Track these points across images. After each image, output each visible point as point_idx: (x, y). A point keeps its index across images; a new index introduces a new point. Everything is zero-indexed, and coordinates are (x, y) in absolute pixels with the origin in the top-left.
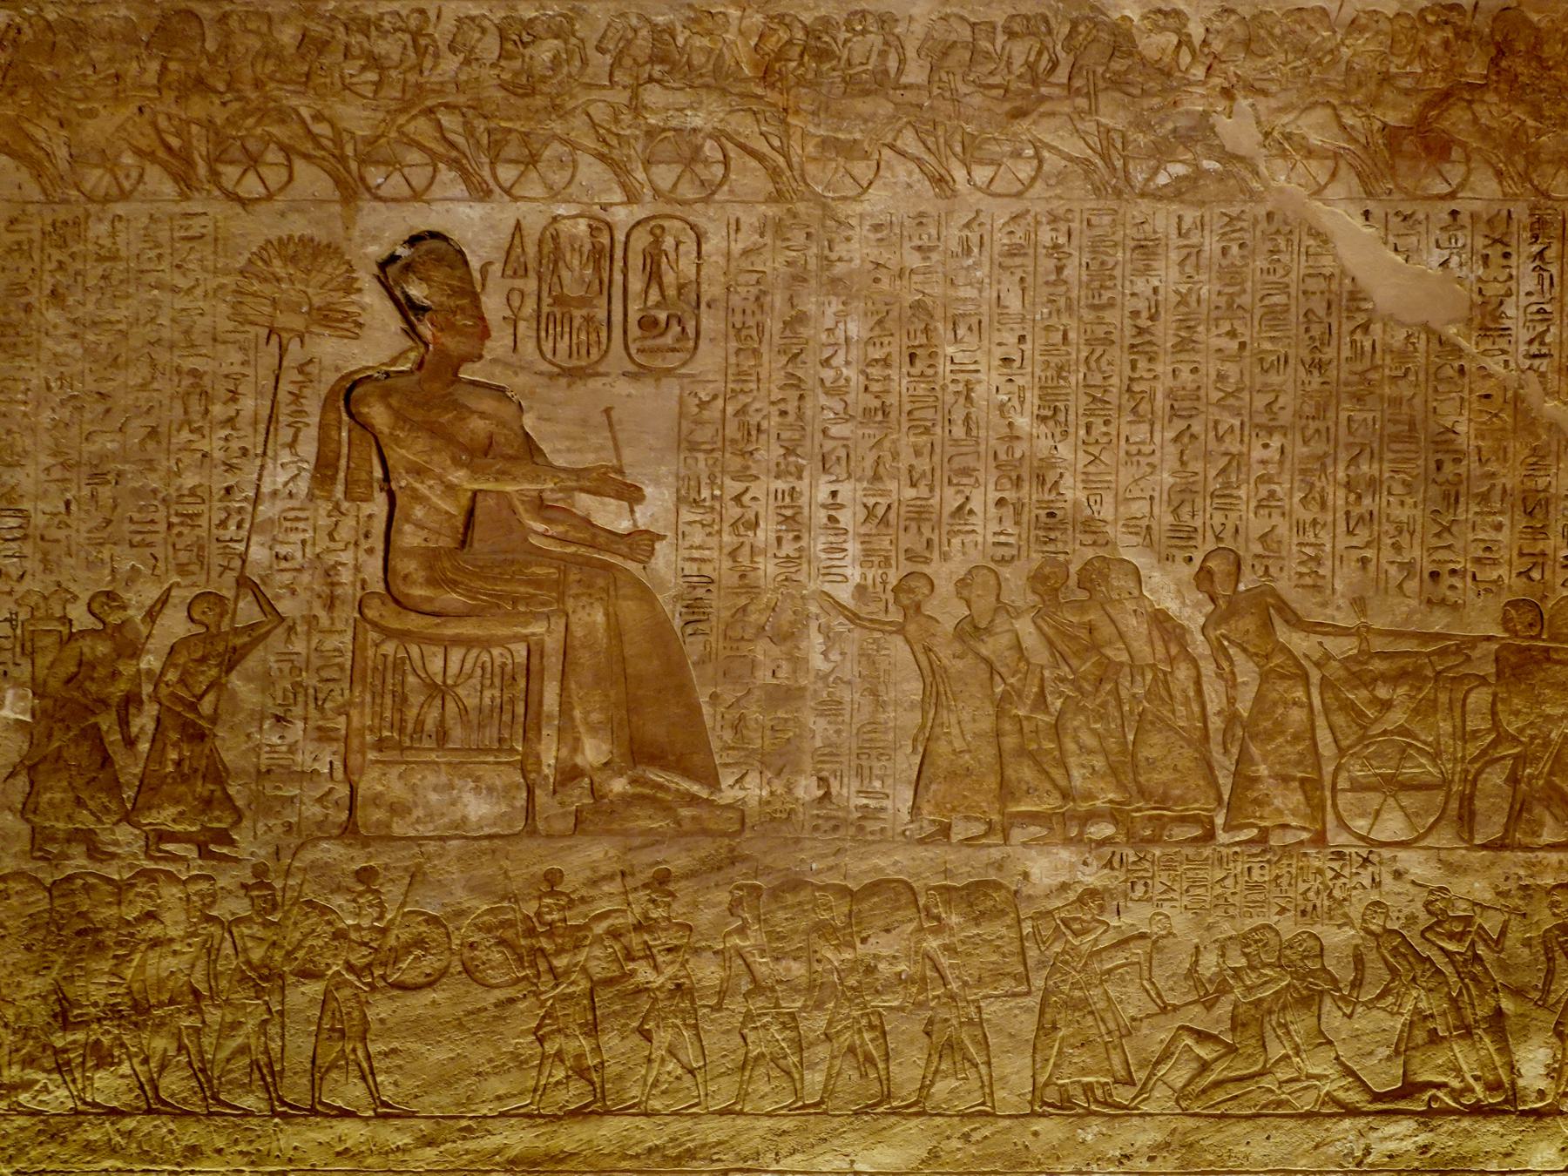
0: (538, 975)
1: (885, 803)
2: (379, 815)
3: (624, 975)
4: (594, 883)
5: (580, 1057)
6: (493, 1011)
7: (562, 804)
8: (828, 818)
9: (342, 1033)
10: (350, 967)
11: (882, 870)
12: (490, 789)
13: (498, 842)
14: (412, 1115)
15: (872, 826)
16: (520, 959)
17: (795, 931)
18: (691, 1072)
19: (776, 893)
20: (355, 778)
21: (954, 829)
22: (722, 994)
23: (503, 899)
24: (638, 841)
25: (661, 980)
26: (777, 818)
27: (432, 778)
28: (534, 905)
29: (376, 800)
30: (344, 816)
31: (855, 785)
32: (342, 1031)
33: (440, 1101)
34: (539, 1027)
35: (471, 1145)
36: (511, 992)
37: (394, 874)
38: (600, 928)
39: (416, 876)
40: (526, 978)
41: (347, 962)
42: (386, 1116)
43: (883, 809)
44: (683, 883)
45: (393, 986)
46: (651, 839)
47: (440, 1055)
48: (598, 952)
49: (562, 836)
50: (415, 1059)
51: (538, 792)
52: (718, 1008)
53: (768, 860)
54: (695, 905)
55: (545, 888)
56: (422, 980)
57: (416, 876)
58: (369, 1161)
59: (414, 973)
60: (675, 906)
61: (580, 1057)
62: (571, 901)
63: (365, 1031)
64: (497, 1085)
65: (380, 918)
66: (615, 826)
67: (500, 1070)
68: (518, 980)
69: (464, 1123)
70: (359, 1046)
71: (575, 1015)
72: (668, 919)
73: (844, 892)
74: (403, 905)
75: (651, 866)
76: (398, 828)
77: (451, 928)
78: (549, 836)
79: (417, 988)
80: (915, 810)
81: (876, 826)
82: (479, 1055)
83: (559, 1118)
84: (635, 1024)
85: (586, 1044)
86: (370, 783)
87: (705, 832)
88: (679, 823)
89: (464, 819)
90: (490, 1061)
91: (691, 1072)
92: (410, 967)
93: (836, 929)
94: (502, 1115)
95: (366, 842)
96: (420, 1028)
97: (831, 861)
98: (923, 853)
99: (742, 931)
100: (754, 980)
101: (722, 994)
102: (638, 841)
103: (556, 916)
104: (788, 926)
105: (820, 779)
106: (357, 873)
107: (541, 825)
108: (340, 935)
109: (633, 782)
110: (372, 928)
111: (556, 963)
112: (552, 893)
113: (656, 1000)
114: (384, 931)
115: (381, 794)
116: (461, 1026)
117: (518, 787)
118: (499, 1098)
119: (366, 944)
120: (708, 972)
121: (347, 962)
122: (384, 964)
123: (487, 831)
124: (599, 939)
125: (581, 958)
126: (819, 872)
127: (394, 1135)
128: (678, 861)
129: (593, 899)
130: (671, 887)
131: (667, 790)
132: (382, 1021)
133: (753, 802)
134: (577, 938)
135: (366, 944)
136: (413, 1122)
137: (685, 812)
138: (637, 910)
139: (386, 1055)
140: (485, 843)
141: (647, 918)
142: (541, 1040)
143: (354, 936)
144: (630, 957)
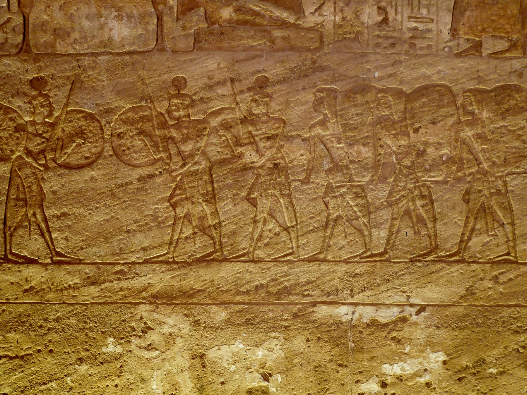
0: (170, 157)
1: (430, 26)
2: (45, 38)
3: (234, 157)
4: (210, 87)
5: (202, 219)
6: (137, 185)
7: (184, 28)
8: (387, 38)
9: (25, 200)
10: (29, 153)
11: (430, 76)
12: (130, 17)
13: (137, 57)
14: (79, 262)
15: (420, 43)
16: (156, 145)
17: (364, 124)
18: (286, 229)
19: (350, 94)
20: (27, 11)
21: (485, 46)
22: (309, 171)
23: (142, 99)
24: (242, 56)
25: (263, 160)
26: (348, 38)
27: (85, 10)
28: (166, 104)
29: (43, 26)
30: (20, 39)
31: (407, 12)
32: (25, 200)
33: (99, 252)
34: (172, 196)
35: (124, 284)
36: (150, 170)
37: (59, 82)
38: (215, 122)
39: (75, 84)
40: (161, 159)
41: (26, 149)
42: (60, 263)
43: (429, 31)
44: (278, 87)
45: (60, 166)
46: (252, 53)
47: (99, 217)
48: (214, 140)
49: (186, 52)
50: (80, 221)
51: (165, 19)
52: (306, 181)
53: (342, 70)
54: (287, 103)
55: (173, 91)
56: (83, 161)
57: (75, 84)
58: (49, 296)
59: (76, 157)
60: (272, 104)
61: (202, 219)
62: (193, 101)
63: (42, 200)
64: (141, 240)
65: (50, 115)
66: (225, 45)
67: (144, 229)
68: (155, 161)
69: (118, 268)
70: (38, 211)
71: (200, 187)
72: (267, 114)
73: (399, 93)
74: (67, 105)
75: (253, 74)
76: (61, 47)
77: (103, 122)
78: (175, 52)
79: (80, 167)
80: (454, 32)
81: (424, 44)
82: (128, 217)
83: (189, 264)
84: (244, 194)
85: (207, 209)
86: (38, 14)
87: (293, 48)
88: (273, 42)
89: (110, 39)
90: (136, 221)
91: (286, 229)
92: (73, 152)
93: (394, 123)
94: (146, 262)
95: (36, 60)
96: (83, 198)
97: (390, 70)
98: (459, 63)
99: (323, 123)
100: (333, 161)
101: (309, 171)
102: (242, 56)
103: (182, 113)
104: (358, 119)
105: (379, 8)
106: (31, 82)
107: (168, 45)
108: (20, 129)
109: (237, 10)
110: (44, 123)
111: (182, 148)
112: (179, 95)
113: (259, 175)
114: (53, 125)
115: (47, 22)
116: (113, 195)
117: (150, 15)
118: (144, 249)
119: (40, 135)
120: (298, 155)
121: (26, 149)
122: (54, 150)
123: (128, 48)
124: (216, 130)
125: (202, 144)
126: (380, 79)
127: (66, 277)
128: (273, 70)
129: (210, 99)
130: (269, 90)
131: (263, 17)
132: (54, 193)
133: (329, 26)
134: (199, 130)
135: (40, 135)
136: (80, 267)
137: (278, 33)
138: (244, 107)
139: (58, 217)
140: (127, 58)
141: (251, 114)
142: (174, 206)
143: (30, 129)
144: (238, 143)
